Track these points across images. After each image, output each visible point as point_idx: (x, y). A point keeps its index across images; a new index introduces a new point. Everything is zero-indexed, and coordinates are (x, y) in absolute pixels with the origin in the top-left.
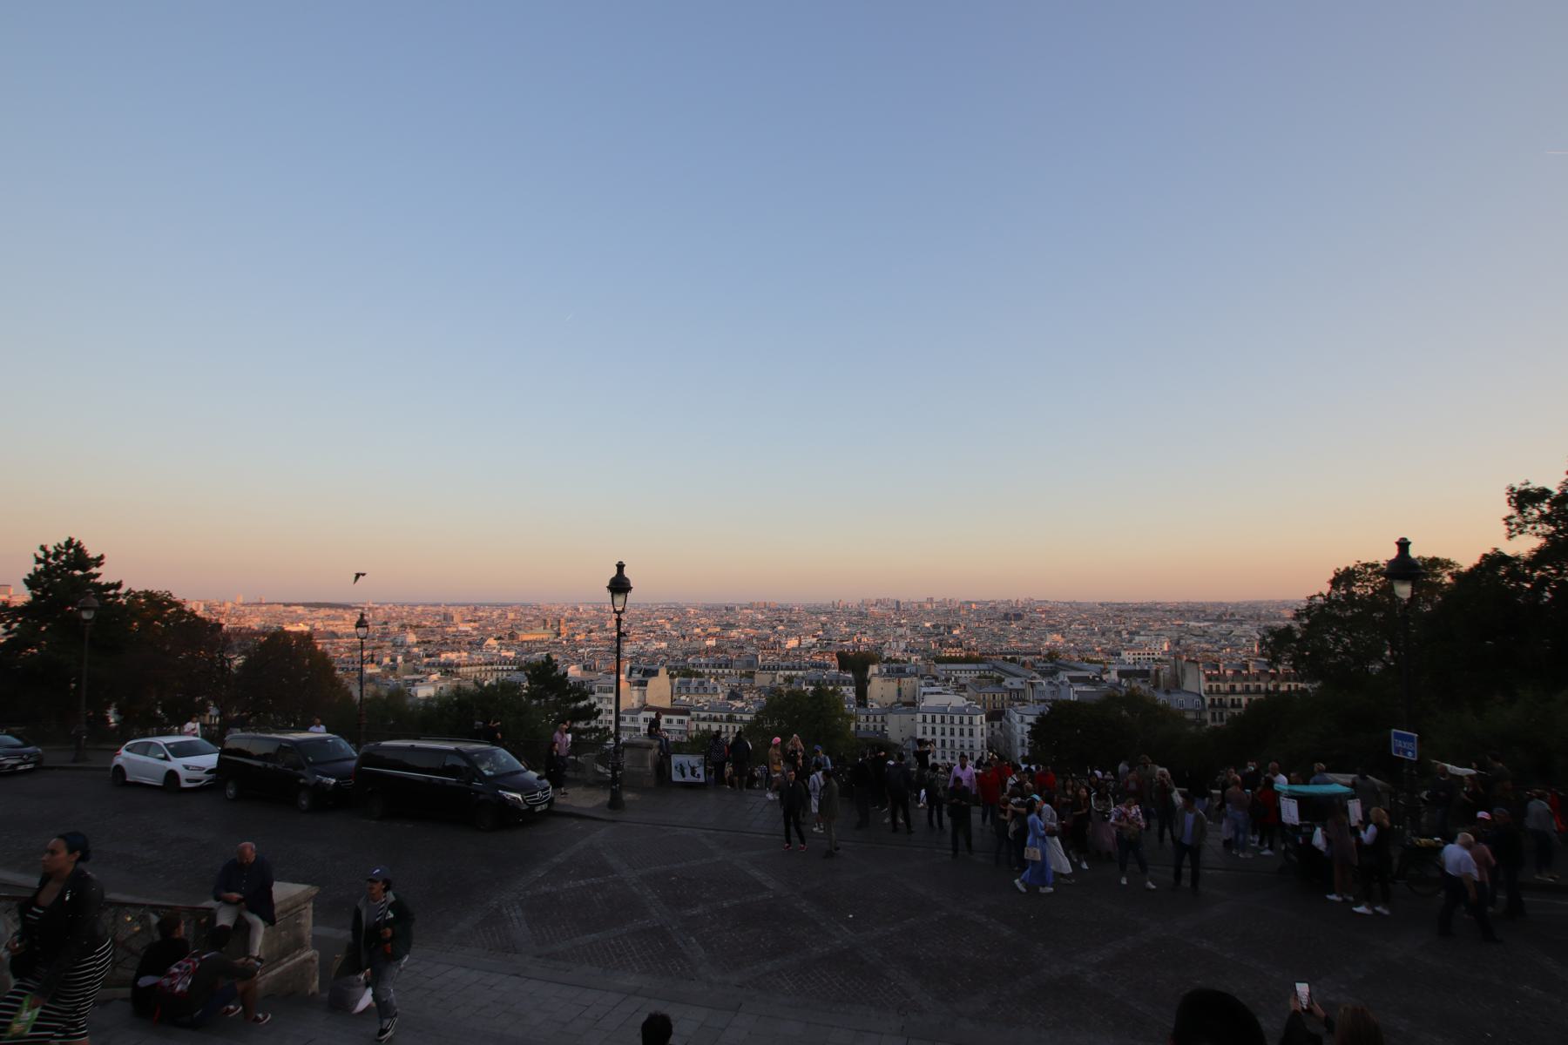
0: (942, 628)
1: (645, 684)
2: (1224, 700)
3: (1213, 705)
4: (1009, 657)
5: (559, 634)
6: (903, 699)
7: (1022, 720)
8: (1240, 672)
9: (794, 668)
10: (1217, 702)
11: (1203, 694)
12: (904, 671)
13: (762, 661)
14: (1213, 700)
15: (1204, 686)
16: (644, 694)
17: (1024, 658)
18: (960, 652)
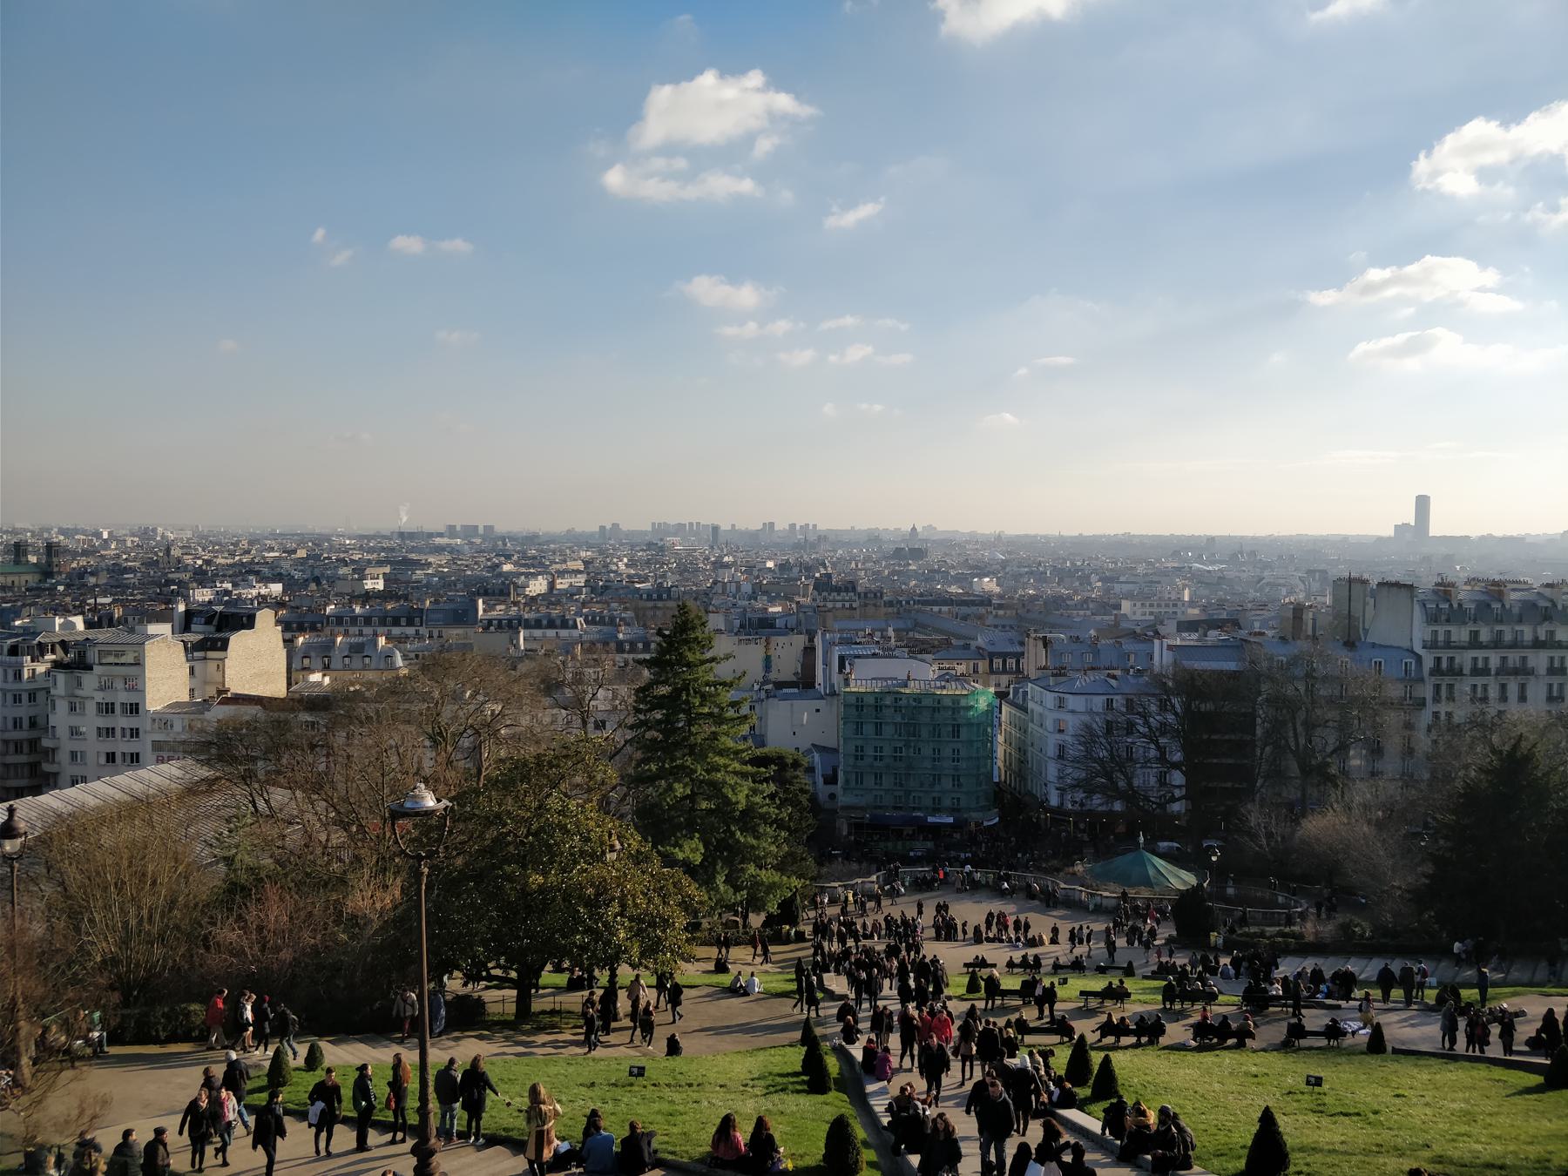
0: (796, 570)
1: (224, 646)
2: (1457, 661)
3: (1437, 671)
4: (936, 609)
5: (49, 574)
6: (773, 676)
7: (1061, 705)
8: (1489, 606)
9: (551, 624)
10: (1444, 665)
11: (1418, 649)
12: (772, 626)
13: (484, 610)
14: (1438, 660)
15: (1420, 633)
16: (221, 669)
17: (964, 610)
18: (850, 600)
